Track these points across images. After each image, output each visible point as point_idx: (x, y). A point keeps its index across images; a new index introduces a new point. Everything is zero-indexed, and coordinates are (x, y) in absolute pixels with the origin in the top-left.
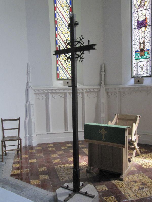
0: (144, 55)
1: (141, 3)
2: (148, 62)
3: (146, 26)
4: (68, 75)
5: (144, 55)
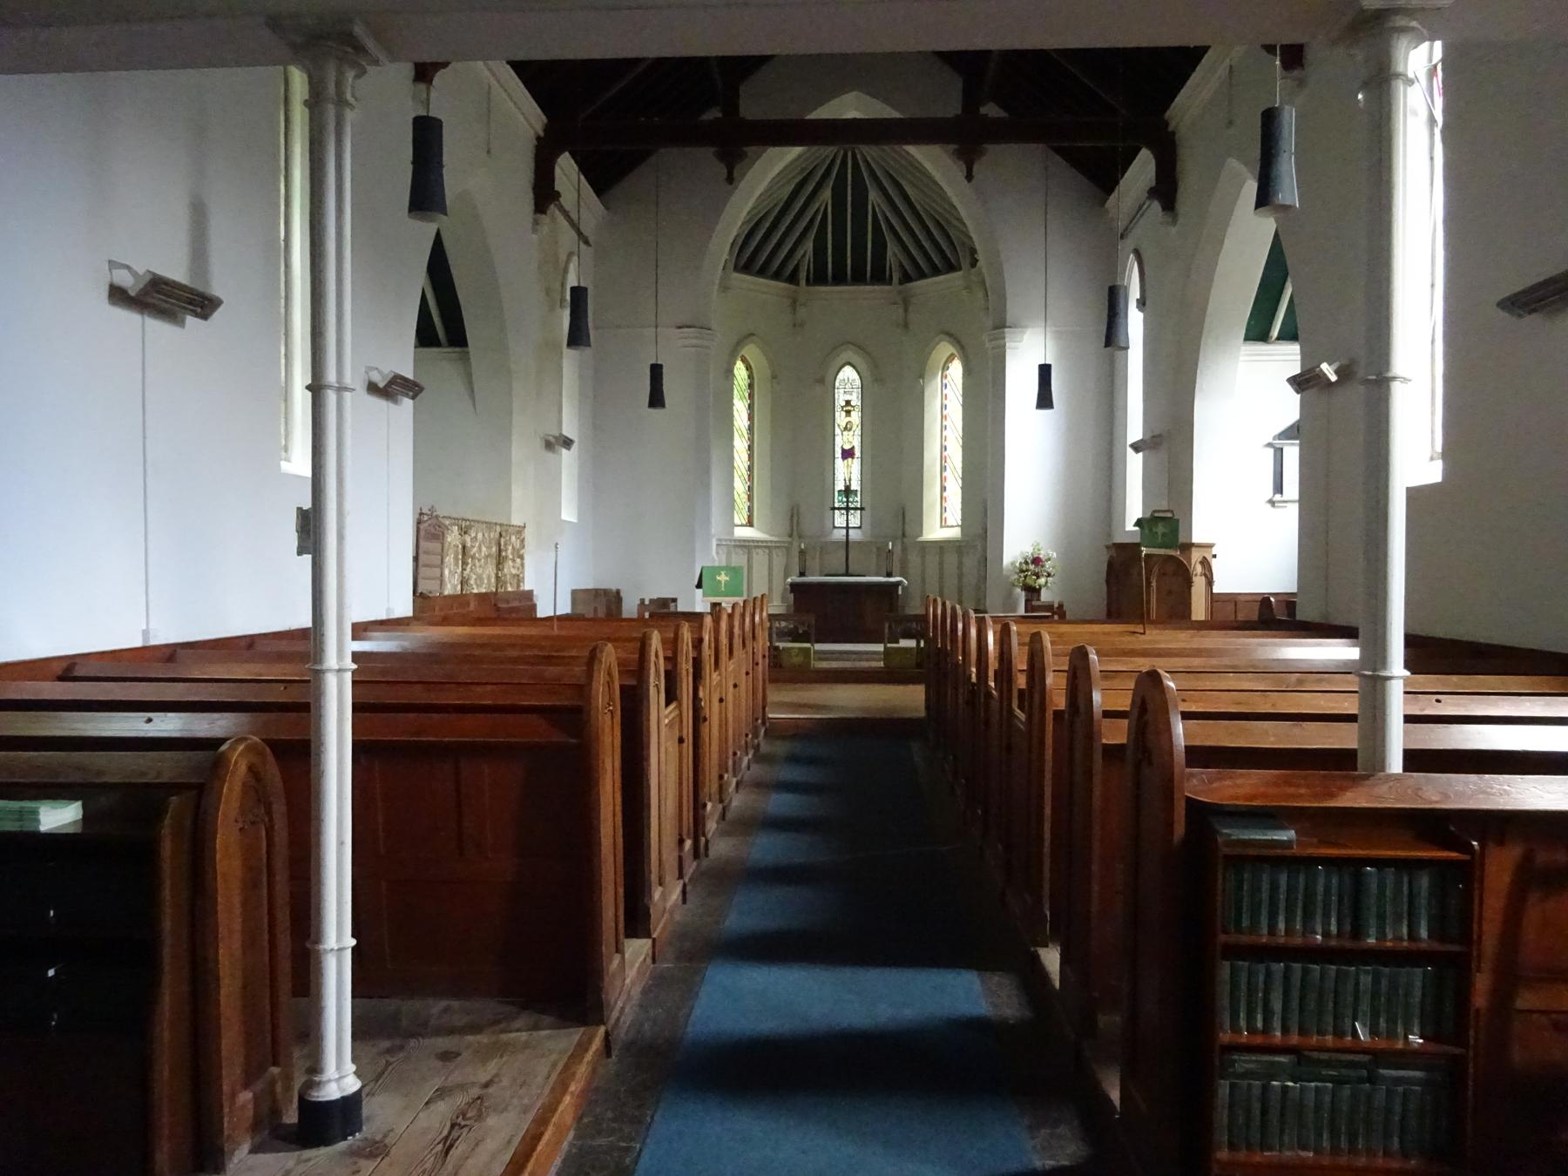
3: (853, 458)
4: (742, 518)
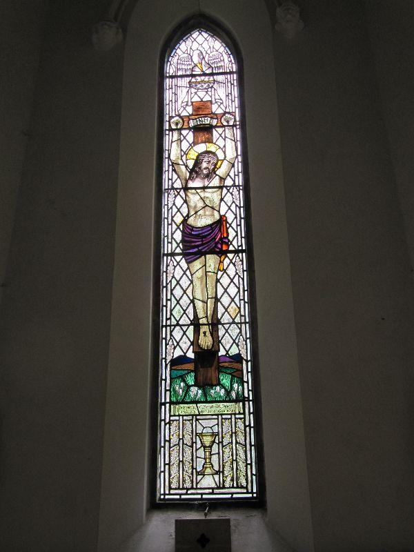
0: (219, 384)
1: (198, 162)
2: (240, 424)
5: (215, 383)
